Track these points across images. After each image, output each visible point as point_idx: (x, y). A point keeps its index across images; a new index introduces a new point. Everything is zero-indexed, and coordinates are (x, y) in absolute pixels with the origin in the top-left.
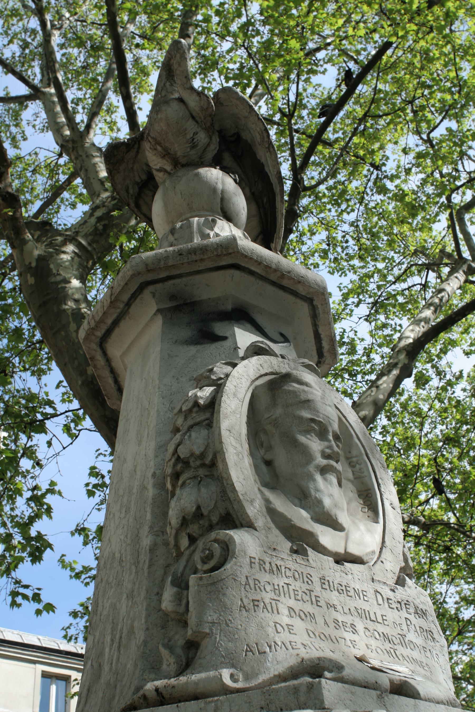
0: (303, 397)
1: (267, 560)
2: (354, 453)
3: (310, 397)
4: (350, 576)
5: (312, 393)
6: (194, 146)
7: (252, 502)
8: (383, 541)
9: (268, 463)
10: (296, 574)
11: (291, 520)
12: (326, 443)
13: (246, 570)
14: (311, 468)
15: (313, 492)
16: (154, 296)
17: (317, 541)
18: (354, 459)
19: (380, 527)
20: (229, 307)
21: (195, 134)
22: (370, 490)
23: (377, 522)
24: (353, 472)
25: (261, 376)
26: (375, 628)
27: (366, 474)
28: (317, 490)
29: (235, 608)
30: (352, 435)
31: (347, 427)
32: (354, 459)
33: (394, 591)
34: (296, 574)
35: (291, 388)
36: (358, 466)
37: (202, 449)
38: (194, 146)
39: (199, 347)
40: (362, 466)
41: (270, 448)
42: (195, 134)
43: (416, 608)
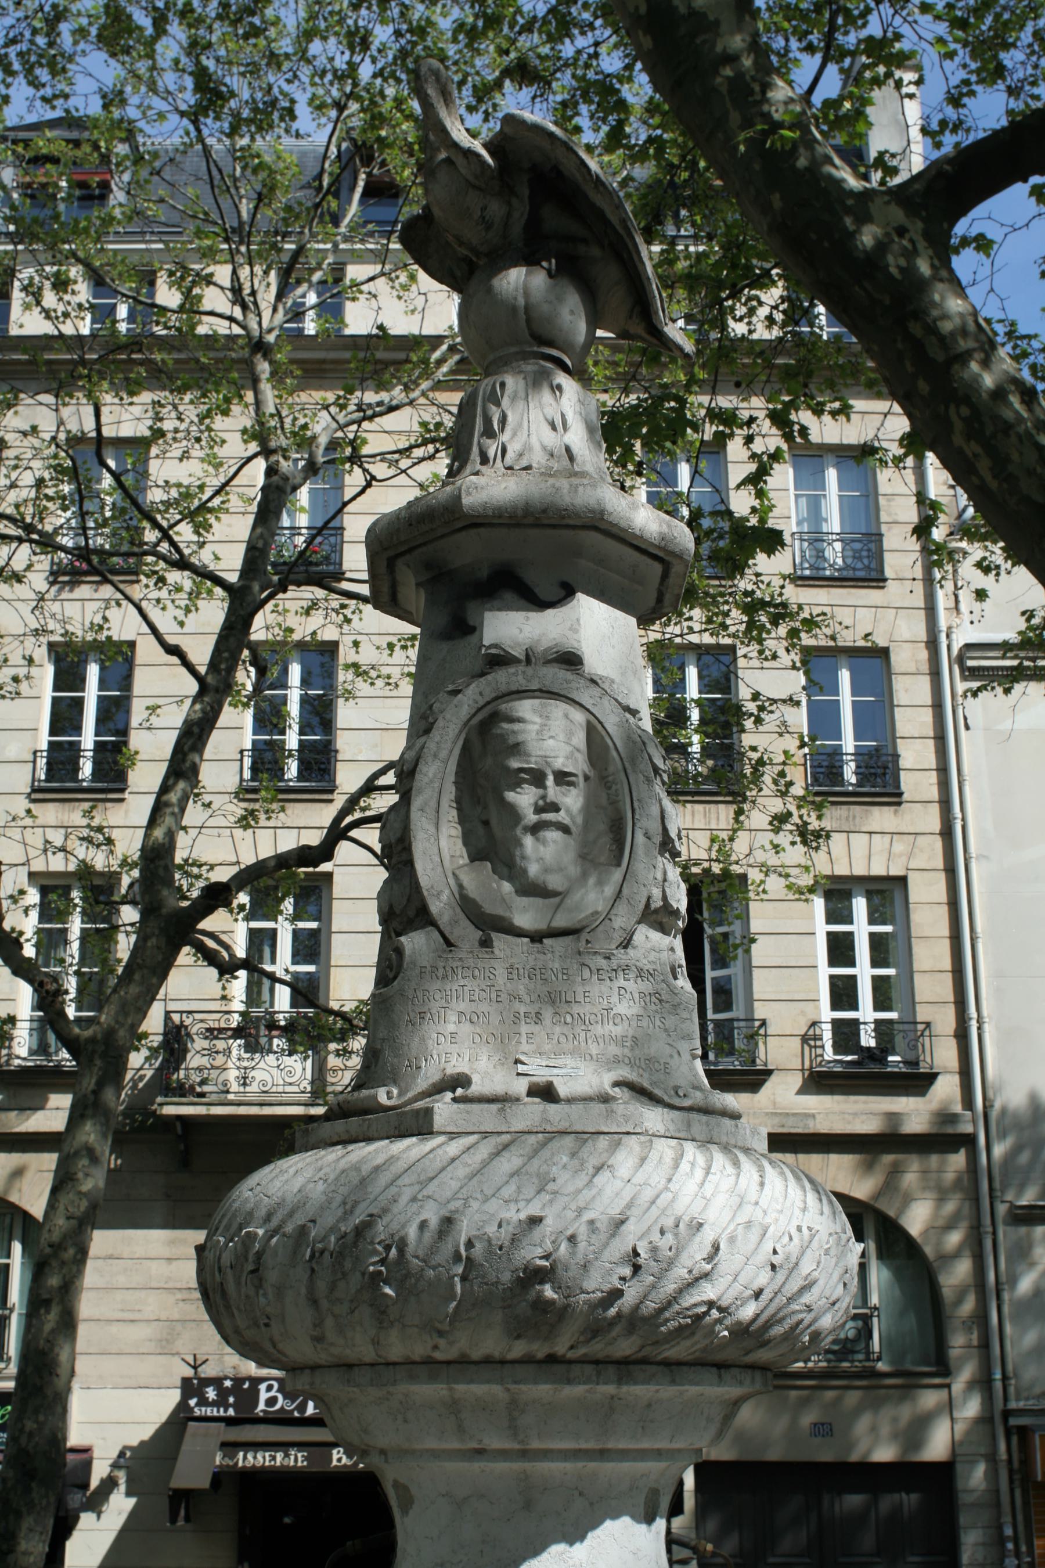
2: (611, 769)
3: (520, 738)
5: (523, 731)
6: (489, 227)
12: (541, 791)
14: (519, 831)
17: (512, 924)
19: (617, 875)
20: (484, 573)
21: (484, 209)
23: (619, 865)
25: (479, 709)
30: (607, 747)
38: (489, 227)
41: (485, 807)
42: (484, 209)
43: (640, 970)
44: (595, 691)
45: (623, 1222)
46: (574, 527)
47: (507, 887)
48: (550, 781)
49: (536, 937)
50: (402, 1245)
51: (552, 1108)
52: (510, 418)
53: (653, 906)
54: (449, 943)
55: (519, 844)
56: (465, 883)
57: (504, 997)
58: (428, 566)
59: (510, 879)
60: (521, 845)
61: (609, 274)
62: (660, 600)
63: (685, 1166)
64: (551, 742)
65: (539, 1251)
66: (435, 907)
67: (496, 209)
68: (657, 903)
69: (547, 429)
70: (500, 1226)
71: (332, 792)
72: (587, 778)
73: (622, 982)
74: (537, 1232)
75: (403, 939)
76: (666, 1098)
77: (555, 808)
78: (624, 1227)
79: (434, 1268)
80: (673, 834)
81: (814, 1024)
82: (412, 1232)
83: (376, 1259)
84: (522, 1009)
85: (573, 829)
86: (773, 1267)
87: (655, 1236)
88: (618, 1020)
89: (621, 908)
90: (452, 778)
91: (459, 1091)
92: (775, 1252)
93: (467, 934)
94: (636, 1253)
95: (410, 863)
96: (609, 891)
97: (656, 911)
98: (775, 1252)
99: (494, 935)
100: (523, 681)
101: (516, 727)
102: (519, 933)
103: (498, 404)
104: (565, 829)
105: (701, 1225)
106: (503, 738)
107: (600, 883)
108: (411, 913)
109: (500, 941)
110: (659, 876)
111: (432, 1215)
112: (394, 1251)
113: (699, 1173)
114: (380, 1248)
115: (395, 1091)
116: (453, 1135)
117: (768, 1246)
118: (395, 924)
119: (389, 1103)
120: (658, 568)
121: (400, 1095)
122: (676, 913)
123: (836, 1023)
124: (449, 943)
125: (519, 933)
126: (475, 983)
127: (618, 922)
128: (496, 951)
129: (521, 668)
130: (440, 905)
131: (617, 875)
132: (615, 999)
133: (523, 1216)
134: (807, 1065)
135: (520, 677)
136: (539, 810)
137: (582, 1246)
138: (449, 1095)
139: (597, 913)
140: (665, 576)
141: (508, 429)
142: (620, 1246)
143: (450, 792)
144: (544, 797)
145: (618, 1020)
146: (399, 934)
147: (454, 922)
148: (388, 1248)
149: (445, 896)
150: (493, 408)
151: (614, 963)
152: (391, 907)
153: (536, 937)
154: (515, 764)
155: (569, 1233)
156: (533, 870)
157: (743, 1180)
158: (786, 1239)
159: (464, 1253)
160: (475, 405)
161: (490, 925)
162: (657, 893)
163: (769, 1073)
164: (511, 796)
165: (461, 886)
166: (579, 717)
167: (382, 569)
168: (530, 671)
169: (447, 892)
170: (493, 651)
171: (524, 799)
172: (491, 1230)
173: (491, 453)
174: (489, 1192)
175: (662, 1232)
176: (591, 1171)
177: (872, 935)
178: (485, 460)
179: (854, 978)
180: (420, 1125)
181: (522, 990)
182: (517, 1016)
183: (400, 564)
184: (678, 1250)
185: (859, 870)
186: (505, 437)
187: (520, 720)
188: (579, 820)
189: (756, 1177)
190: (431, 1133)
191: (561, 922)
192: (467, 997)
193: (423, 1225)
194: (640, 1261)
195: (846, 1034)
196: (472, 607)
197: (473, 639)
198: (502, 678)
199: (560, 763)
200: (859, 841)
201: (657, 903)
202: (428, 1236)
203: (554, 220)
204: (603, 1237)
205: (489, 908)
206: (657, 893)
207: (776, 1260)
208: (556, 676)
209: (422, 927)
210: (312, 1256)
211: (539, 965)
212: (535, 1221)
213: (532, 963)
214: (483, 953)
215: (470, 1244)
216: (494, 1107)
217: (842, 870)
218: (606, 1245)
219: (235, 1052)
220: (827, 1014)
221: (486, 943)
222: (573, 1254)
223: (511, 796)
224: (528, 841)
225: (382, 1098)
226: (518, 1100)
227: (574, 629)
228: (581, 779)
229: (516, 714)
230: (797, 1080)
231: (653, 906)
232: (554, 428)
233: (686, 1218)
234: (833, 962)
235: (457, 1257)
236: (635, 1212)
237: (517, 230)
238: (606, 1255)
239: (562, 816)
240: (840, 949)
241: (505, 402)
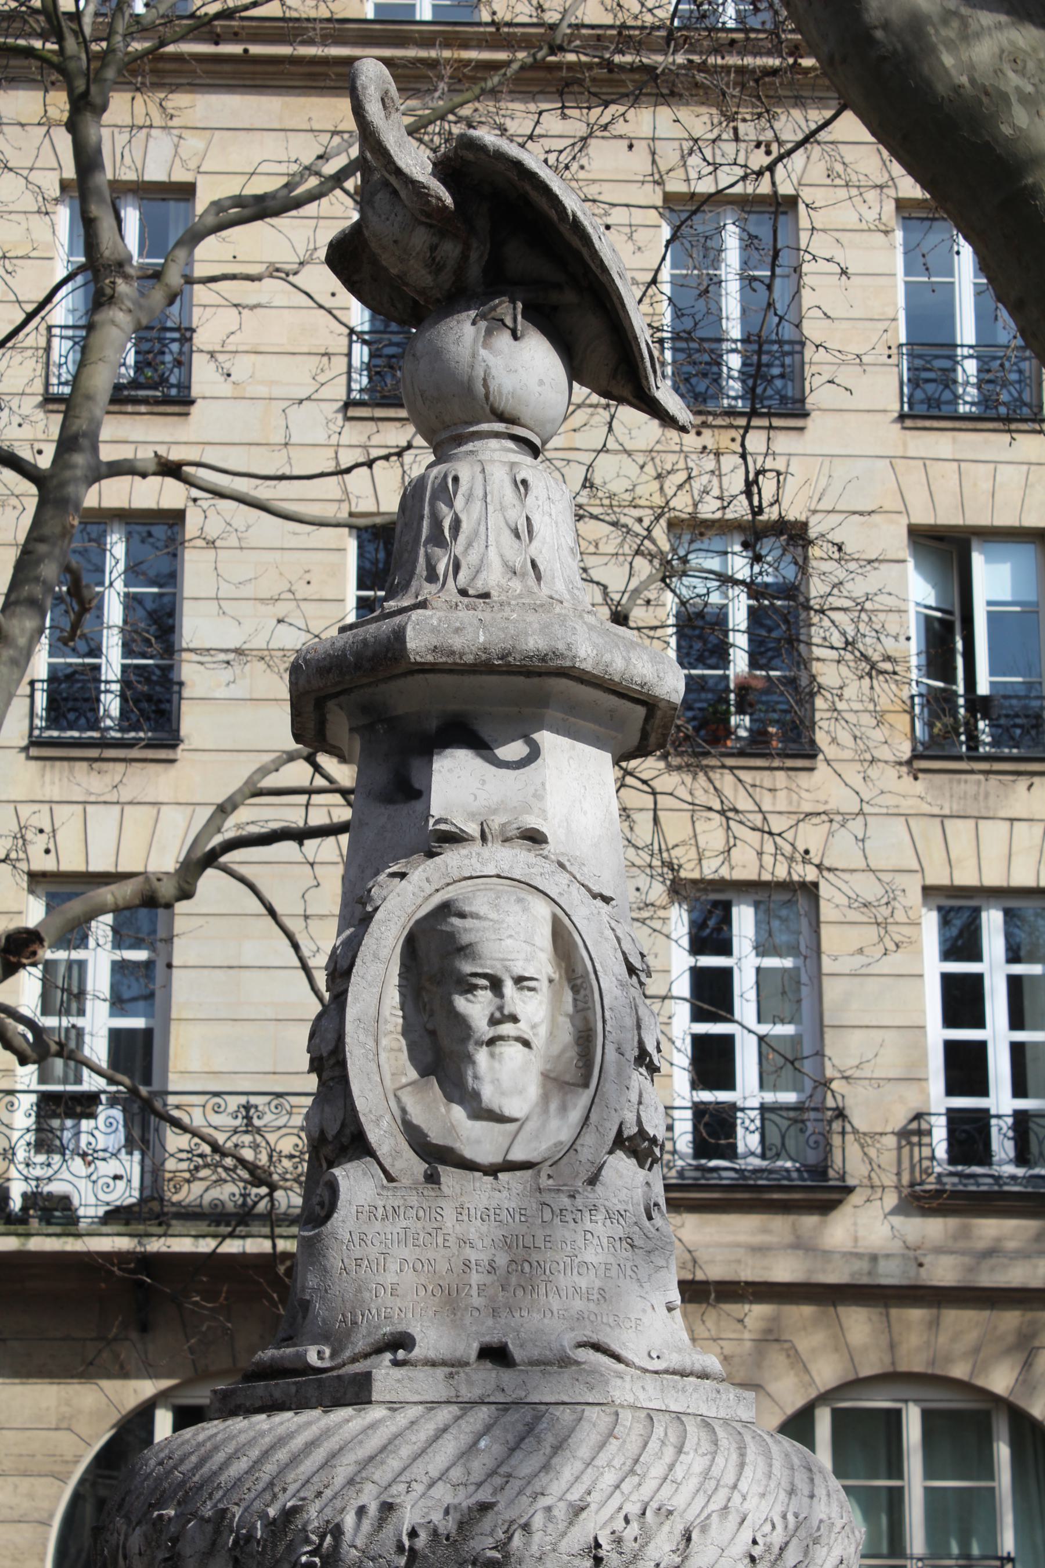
0: (465, 939)
1: (380, 1203)
2: (579, 971)
4: (505, 1193)
7: (377, 1121)
8: (587, 1118)
9: (432, 1033)
10: (421, 1213)
11: (426, 1136)
12: (497, 1001)
13: (351, 1224)
15: (470, 1080)
16: (341, 708)
18: (579, 982)
20: (433, 724)
22: (590, 1030)
23: (586, 1085)
24: (575, 1000)
26: (527, 1257)
27: (590, 1004)
28: (476, 1077)
29: (336, 1273)
31: (570, 933)
32: (579, 982)
33: (574, 1197)
34: (421, 1213)
35: (448, 929)
36: (582, 992)
37: (331, 1047)
39: (392, 808)
40: (588, 992)
44: (563, 878)
45: (583, 1509)
46: (540, 674)
47: (458, 1112)
48: (509, 988)
49: (492, 1171)
50: (337, 1531)
51: (507, 1376)
52: (465, 525)
53: (626, 1133)
54: (390, 1179)
55: (470, 1059)
56: (409, 1108)
57: (452, 1241)
58: (366, 709)
59: (461, 1103)
60: (474, 1063)
61: (589, 326)
62: (645, 735)
63: (653, 1445)
64: (509, 941)
65: (490, 1542)
66: (374, 1135)
67: (450, 250)
68: (631, 1130)
69: (507, 536)
70: (447, 1512)
71: (174, 747)
72: (551, 981)
73: (589, 1226)
74: (487, 1522)
75: (337, 1171)
76: (636, 1361)
77: (514, 1019)
78: (584, 1515)
79: (373, 1559)
80: (651, 1048)
81: (918, 1116)
82: (349, 1520)
83: (309, 1548)
84: (473, 1256)
85: (535, 1042)
86: (753, 1559)
87: (619, 1524)
88: (584, 1270)
89: (589, 1139)
90: (396, 981)
91: (401, 1354)
92: (755, 1542)
93: (409, 1165)
94: (598, 1546)
95: (344, 1080)
96: (575, 1115)
97: (630, 1138)
98: (755, 1542)
99: (441, 1168)
100: (478, 866)
101: (468, 923)
102: (470, 1166)
103: (451, 505)
104: (526, 1044)
105: (670, 1513)
106: (451, 937)
107: (563, 1109)
108: (345, 1140)
109: (449, 1176)
110: (634, 1098)
111: (369, 1497)
112: (329, 1539)
113: (669, 1453)
114: (314, 1538)
115: (327, 1352)
116: (394, 1406)
117: (745, 1536)
118: (327, 1150)
119: (318, 1364)
120: (641, 711)
121: (333, 1356)
122: (654, 1141)
123: (952, 1114)
124: (390, 1179)
125: (470, 1166)
126: (419, 1225)
127: (586, 1153)
128: (444, 1187)
129: (477, 847)
130: (382, 1133)
131: (585, 1097)
132: (580, 1242)
133: (472, 1501)
134: (906, 1179)
135: (474, 861)
136: (493, 1022)
137: (537, 1537)
138: (388, 1356)
139: (561, 1143)
140: (647, 719)
141: (462, 538)
142: (580, 1536)
143: (393, 997)
144: (501, 1008)
145: (584, 1270)
146: (331, 1164)
147: (396, 1154)
148: (322, 1538)
149: (386, 1122)
150: (443, 508)
151: (579, 1201)
152: (322, 1132)
153: (492, 1171)
154: (467, 968)
155: (522, 1521)
156: (488, 1095)
157: (720, 1460)
158: (767, 1528)
159: (407, 1544)
160: (422, 500)
161: (437, 1157)
162: (630, 1117)
163: (849, 1190)
164: (461, 1003)
165: (404, 1111)
166: (543, 911)
167: (309, 708)
168: (487, 851)
169: (388, 1117)
170: (443, 827)
171: (476, 1008)
172: (437, 1517)
173: (441, 568)
174: (435, 1474)
175: (627, 1520)
176: (548, 1450)
177: (981, 1024)
178: (432, 576)
179: (982, 1045)
180: (356, 1392)
181: (473, 1236)
182: (467, 1264)
183: (331, 705)
184: (645, 1538)
185: (993, 878)
186: (458, 548)
187: (475, 916)
188: (543, 1030)
189: (734, 1457)
190: (370, 1402)
191: (518, 1155)
192: (410, 1241)
193: (361, 1511)
194: (602, 1553)
195: (969, 1135)
196: (416, 763)
197: (418, 805)
198: (452, 859)
199: (520, 969)
200: (994, 832)
201: (631, 1130)
202: (367, 1525)
203: (520, 258)
204: (562, 1526)
205: (436, 1137)
206: (630, 1117)
207: (757, 1551)
208: (516, 859)
209: (358, 1158)
210: (236, 1542)
211: (494, 1204)
212: (485, 1508)
213: (485, 1202)
214: (429, 1191)
215: (413, 1534)
216: (441, 1372)
217: (965, 878)
218: (564, 1534)
219: (21, 1154)
220: (938, 1100)
221: (432, 1178)
222: (527, 1544)
223: (461, 1003)
224: (482, 1056)
225: (312, 1357)
226: (467, 1364)
227: (539, 796)
228: (545, 983)
229: (467, 909)
230: (891, 1200)
231: (626, 1133)
232: (517, 536)
233: (654, 1505)
234: (950, 1020)
235: (400, 1548)
236: (595, 1498)
237: (474, 272)
238: (564, 1546)
239: (522, 1028)
240: (962, 1001)
241: (459, 503)
